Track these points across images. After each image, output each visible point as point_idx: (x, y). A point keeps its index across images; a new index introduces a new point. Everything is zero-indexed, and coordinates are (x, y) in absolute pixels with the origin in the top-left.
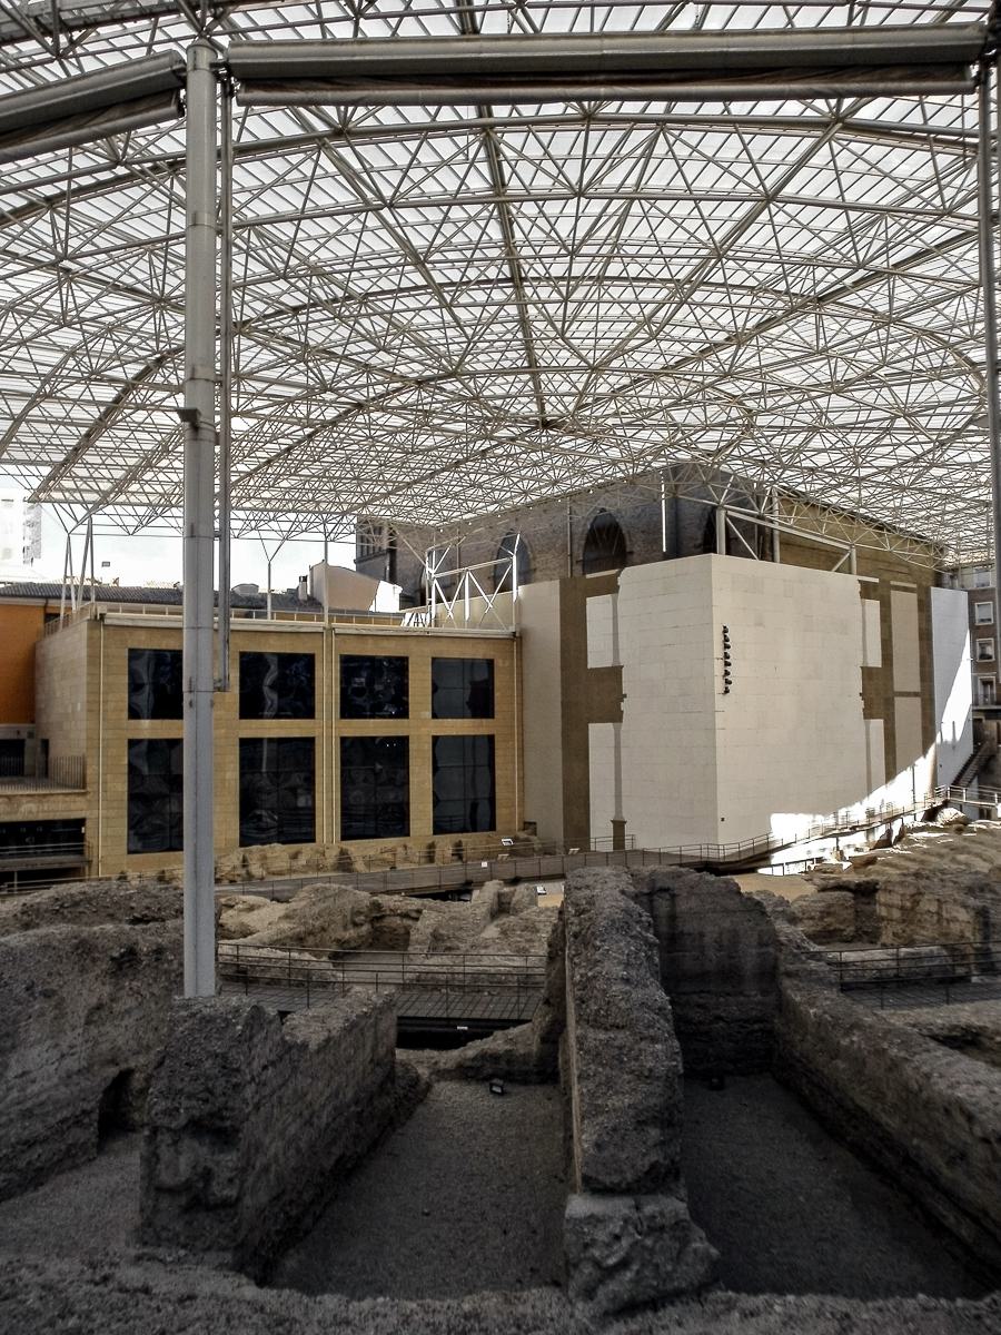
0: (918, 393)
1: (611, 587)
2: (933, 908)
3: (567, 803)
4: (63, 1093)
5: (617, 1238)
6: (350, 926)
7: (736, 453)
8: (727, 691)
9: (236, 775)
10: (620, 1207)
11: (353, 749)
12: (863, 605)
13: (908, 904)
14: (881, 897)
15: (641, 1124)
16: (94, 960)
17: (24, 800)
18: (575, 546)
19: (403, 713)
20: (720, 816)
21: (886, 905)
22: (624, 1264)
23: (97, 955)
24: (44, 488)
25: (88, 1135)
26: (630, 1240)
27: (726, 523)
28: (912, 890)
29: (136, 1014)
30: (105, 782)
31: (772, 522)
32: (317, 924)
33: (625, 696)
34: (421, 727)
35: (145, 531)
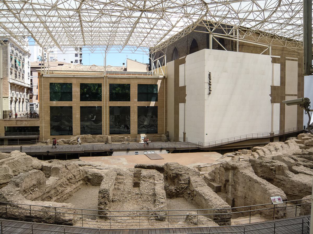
3: (175, 127)
8: (210, 94)
9: (79, 116)
11: (112, 109)
12: (273, 66)
18: (188, 51)
19: (100, 99)
20: (205, 133)
27: (213, 38)
31: (236, 39)
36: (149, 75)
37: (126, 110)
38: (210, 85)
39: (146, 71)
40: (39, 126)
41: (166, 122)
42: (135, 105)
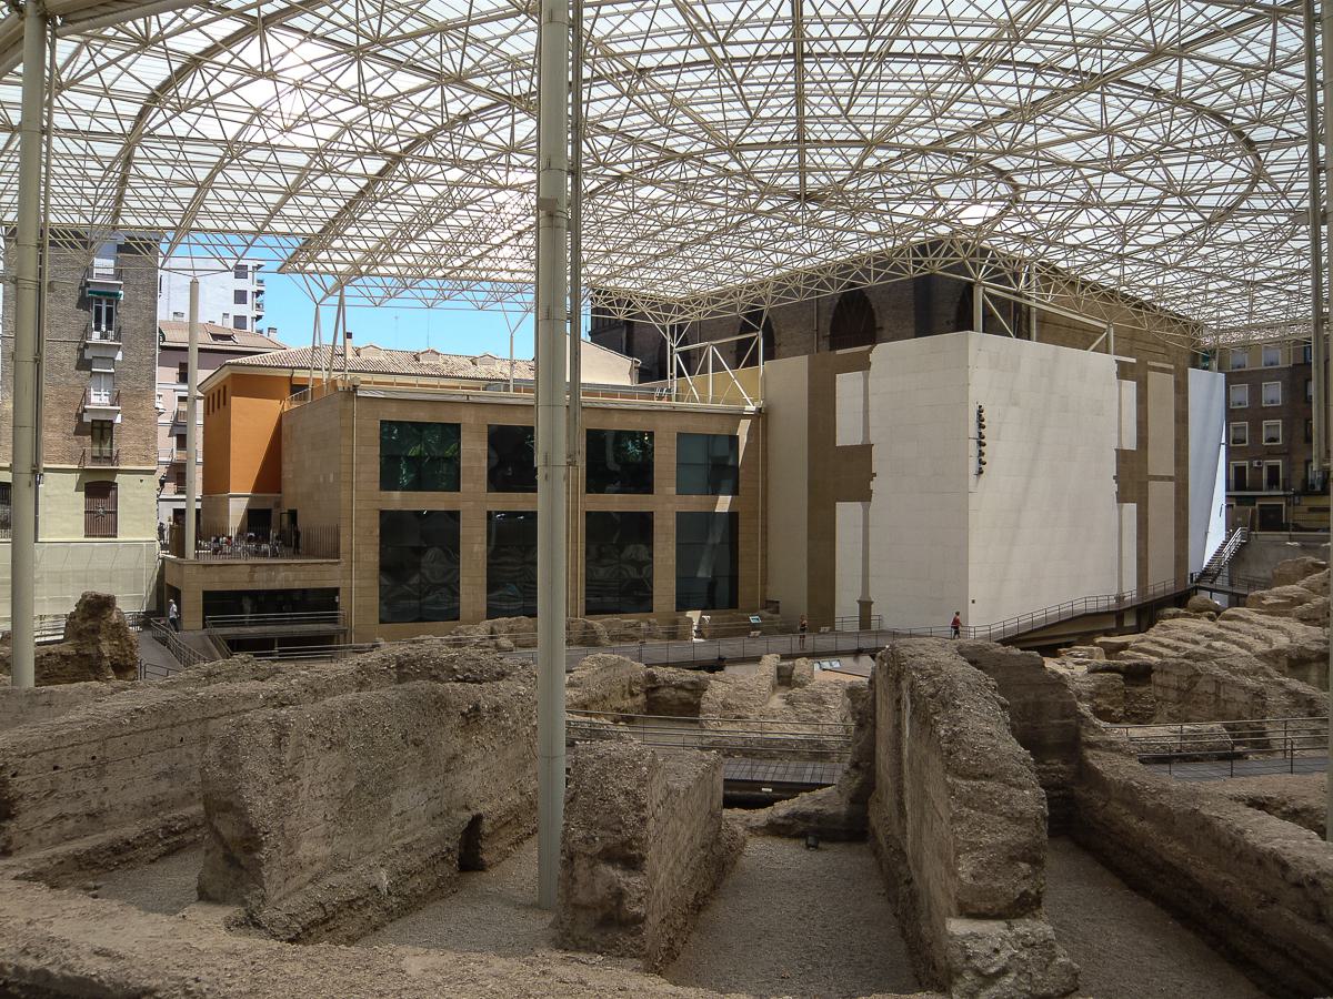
0: (1196, 171)
1: (863, 364)
2: (1211, 689)
4: (432, 831)
5: (996, 951)
6: (627, 696)
7: (998, 228)
8: (981, 472)
10: (995, 928)
11: (598, 526)
12: (1120, 386)
13: (1185, 685)
14: (1157, 678)
15: (1012, 860)
16: (448, 714)
17: (281, 568)
21: (1162, 686)
22: (1003, 972)
23: (450, 709)
24: (292, 260)
25: (445, 871)
26: (1009, 954)
27: (984, 300)
28: (1190, 672)
29: (482, 766)
30: (358, 553)
31: (1029, 298)
32: (600, 692)
33: (875, 475)
34: (666, 503)
35: (393, 302)
36: (660, 398)
37: (641, 526)
38: (981, 444)
39: (626, 382)
40: (329, 585)
41: (782, 568)
42: (669, 506)
